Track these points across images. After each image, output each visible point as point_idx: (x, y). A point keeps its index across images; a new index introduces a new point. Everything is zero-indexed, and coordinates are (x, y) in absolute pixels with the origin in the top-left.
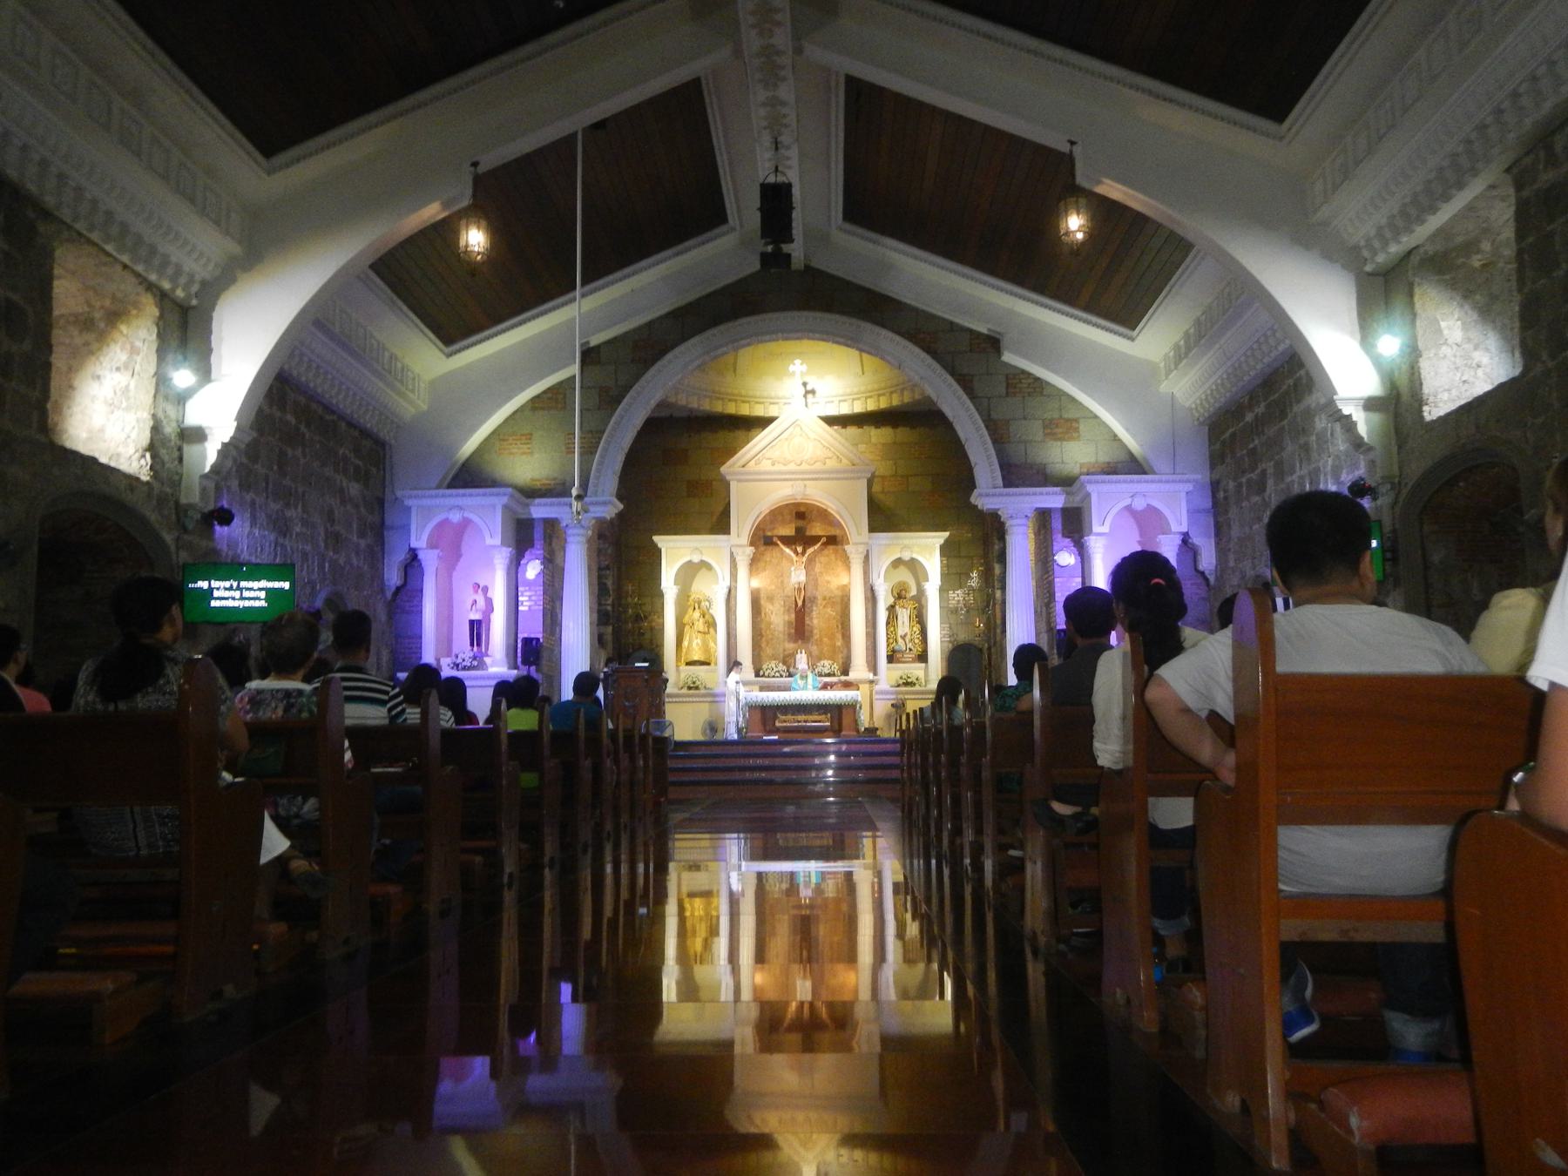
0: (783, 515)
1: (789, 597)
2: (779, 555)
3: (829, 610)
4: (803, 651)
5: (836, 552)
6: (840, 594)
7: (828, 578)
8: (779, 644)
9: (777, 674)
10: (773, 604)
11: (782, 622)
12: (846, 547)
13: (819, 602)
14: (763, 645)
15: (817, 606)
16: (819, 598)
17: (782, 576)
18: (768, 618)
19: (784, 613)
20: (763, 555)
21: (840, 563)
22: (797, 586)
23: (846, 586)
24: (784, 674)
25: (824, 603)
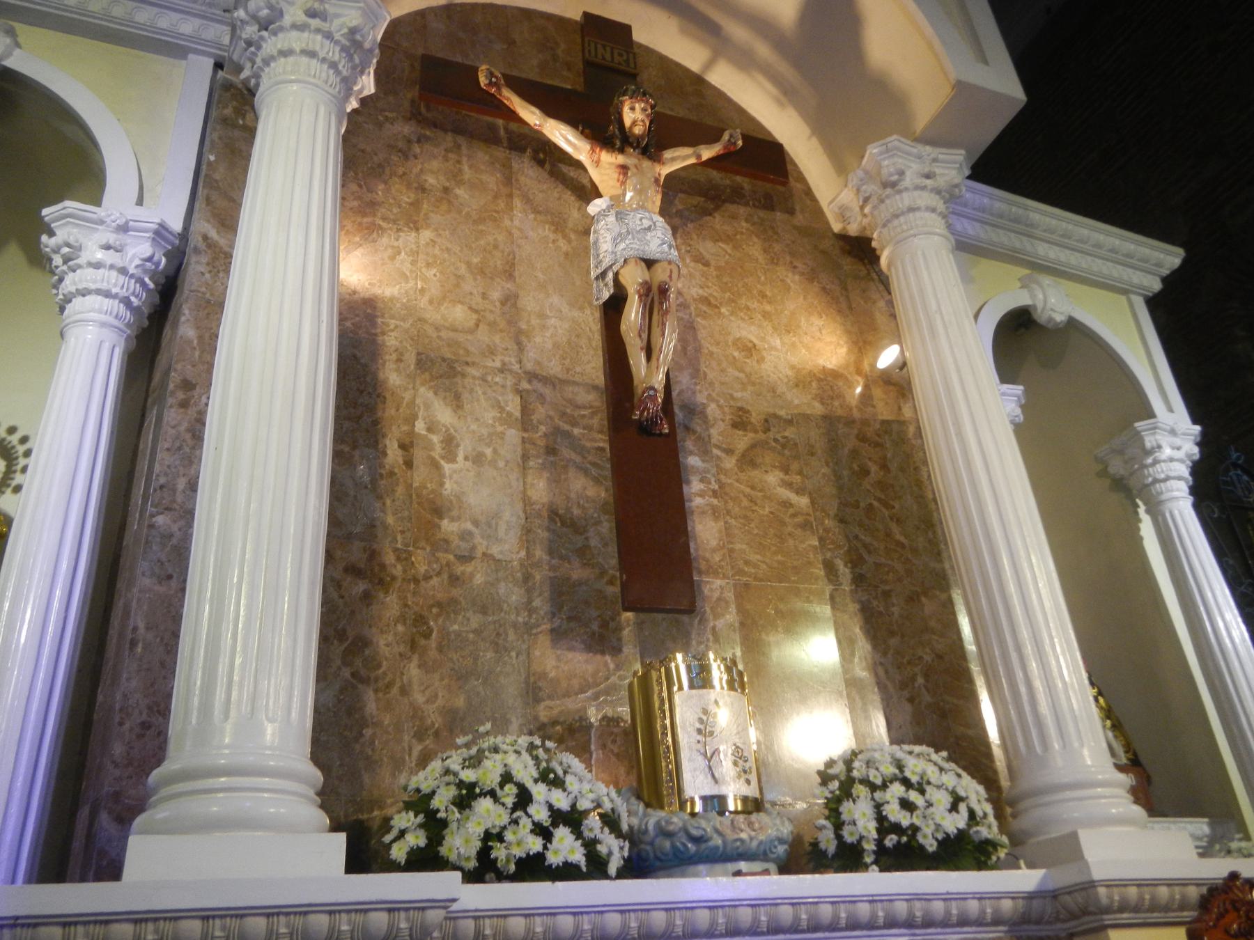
0: (512, 43)
1: (546, 380)
2: (492, 180)
3: (773, 478)
4: (718, 673)
5: (767, 233)
6: (818, 409)
7: (747, 331)
8: (500, 649)
9: (565, 848)
10: (457, 402)
11: (511, 516)
12: (850, 177)
13: (714, 432)
14: (386, 643)
15: (705, 453)
16: (712, 410)
17: (510, 276)
18: (420, 476)
19: (525, 457)
20: (405, 155)
21: (793, 279)
22: (633, 279)
23: (835, 374)
24: (614, 849)
25: (742, 441)
